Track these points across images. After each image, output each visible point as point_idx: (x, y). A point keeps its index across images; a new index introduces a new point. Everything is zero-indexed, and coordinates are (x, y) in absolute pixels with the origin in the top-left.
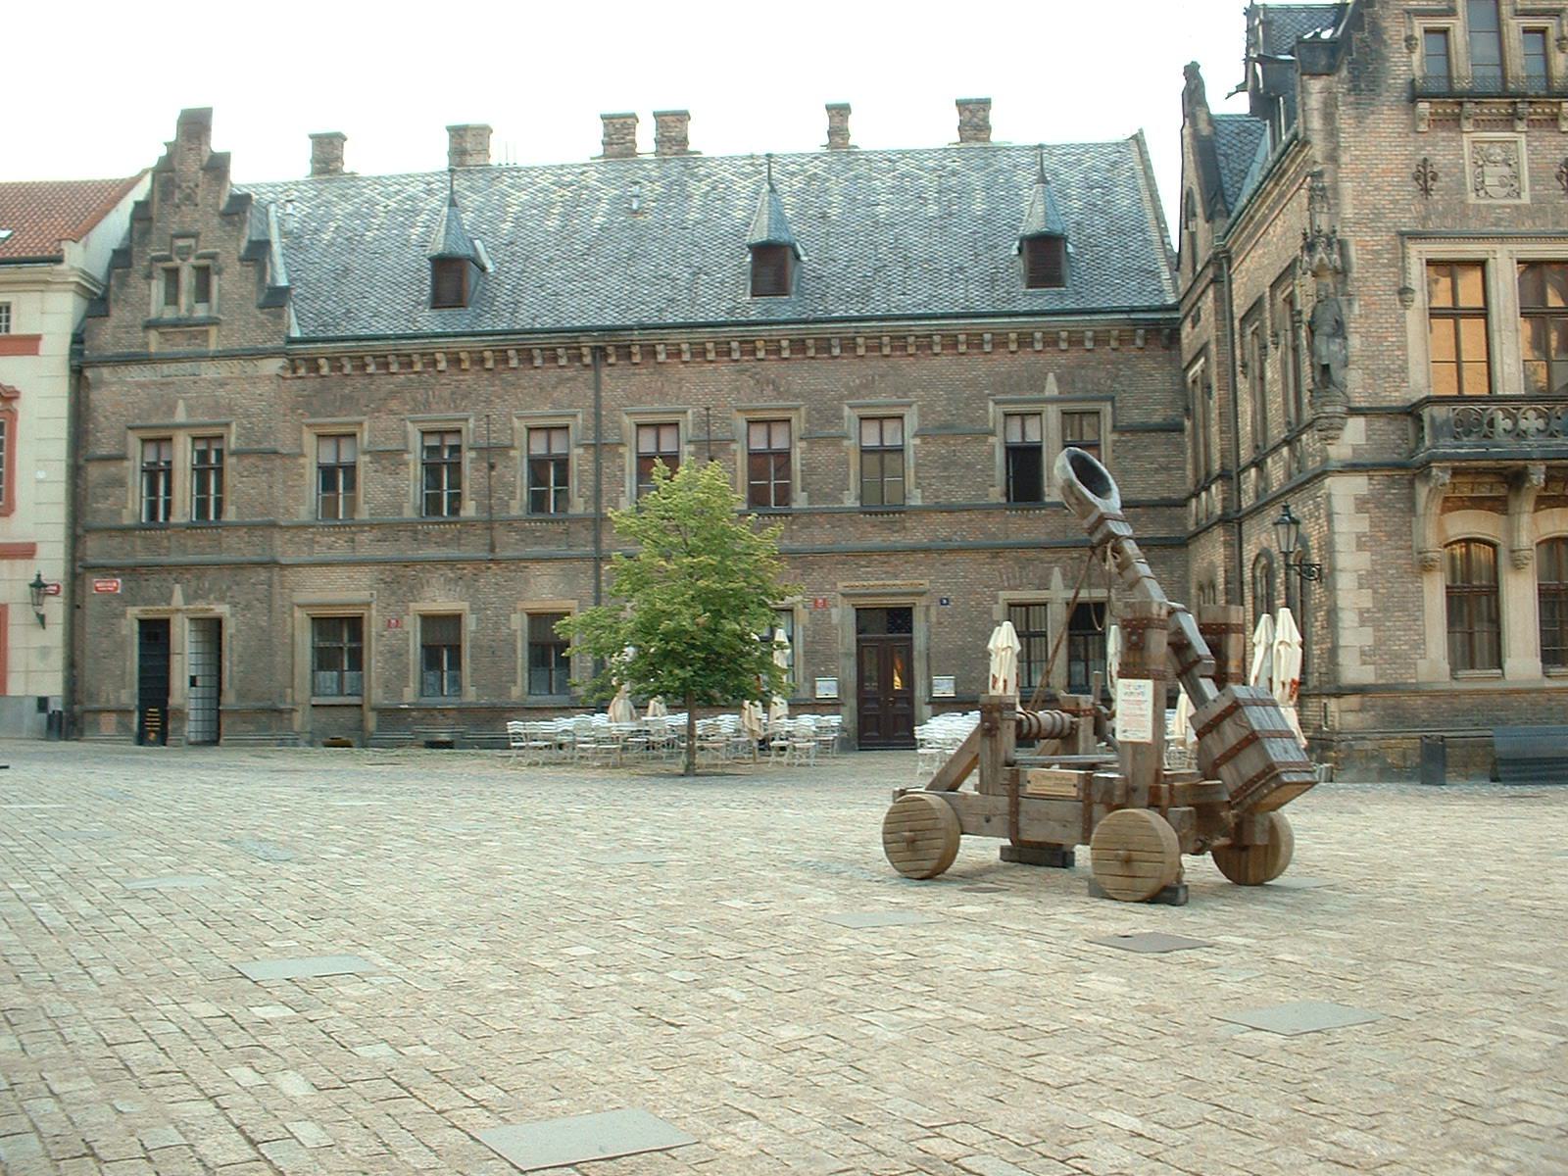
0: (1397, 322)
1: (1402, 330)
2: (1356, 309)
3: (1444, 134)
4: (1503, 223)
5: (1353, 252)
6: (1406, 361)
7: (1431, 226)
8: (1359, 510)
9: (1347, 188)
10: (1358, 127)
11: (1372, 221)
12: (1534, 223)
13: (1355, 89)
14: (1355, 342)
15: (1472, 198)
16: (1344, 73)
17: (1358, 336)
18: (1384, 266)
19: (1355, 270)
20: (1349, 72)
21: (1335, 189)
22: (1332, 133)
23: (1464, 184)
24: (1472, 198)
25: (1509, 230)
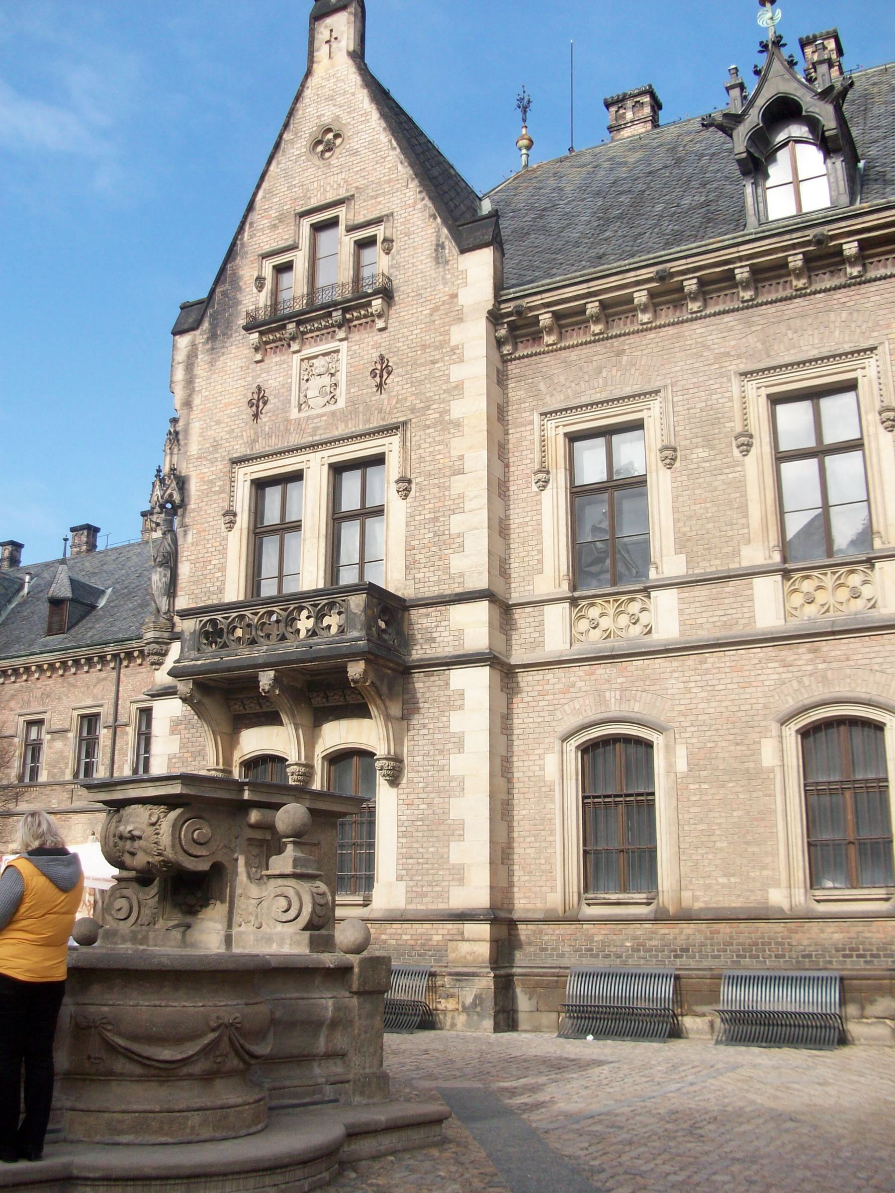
0: (221, 545)
1: (223, 552)
2: (190, 538)
3: (278, 359)
4: (319, 432)
5: (194, 487)
6: (223, 582)
7: (259, 448)
8: (173, 732)
9: (196, 428)
10: (210, 370)
11: (211, 453)
12: (347, 425)
13: (213, 337)
14: (184, 570)
15: (294, 414)
16: (206, 325)
17: (188, 563)
18: (215, 493)
19: (192, 501)
20: (210, 324)
21: (186, 430)
22: (190, 381)
23: (290, 402)
24: (294, 414)
25: (323, 437)
